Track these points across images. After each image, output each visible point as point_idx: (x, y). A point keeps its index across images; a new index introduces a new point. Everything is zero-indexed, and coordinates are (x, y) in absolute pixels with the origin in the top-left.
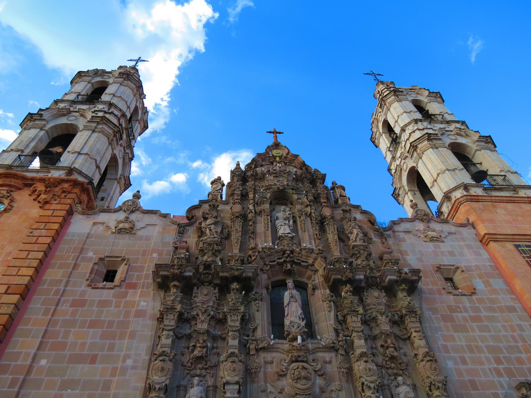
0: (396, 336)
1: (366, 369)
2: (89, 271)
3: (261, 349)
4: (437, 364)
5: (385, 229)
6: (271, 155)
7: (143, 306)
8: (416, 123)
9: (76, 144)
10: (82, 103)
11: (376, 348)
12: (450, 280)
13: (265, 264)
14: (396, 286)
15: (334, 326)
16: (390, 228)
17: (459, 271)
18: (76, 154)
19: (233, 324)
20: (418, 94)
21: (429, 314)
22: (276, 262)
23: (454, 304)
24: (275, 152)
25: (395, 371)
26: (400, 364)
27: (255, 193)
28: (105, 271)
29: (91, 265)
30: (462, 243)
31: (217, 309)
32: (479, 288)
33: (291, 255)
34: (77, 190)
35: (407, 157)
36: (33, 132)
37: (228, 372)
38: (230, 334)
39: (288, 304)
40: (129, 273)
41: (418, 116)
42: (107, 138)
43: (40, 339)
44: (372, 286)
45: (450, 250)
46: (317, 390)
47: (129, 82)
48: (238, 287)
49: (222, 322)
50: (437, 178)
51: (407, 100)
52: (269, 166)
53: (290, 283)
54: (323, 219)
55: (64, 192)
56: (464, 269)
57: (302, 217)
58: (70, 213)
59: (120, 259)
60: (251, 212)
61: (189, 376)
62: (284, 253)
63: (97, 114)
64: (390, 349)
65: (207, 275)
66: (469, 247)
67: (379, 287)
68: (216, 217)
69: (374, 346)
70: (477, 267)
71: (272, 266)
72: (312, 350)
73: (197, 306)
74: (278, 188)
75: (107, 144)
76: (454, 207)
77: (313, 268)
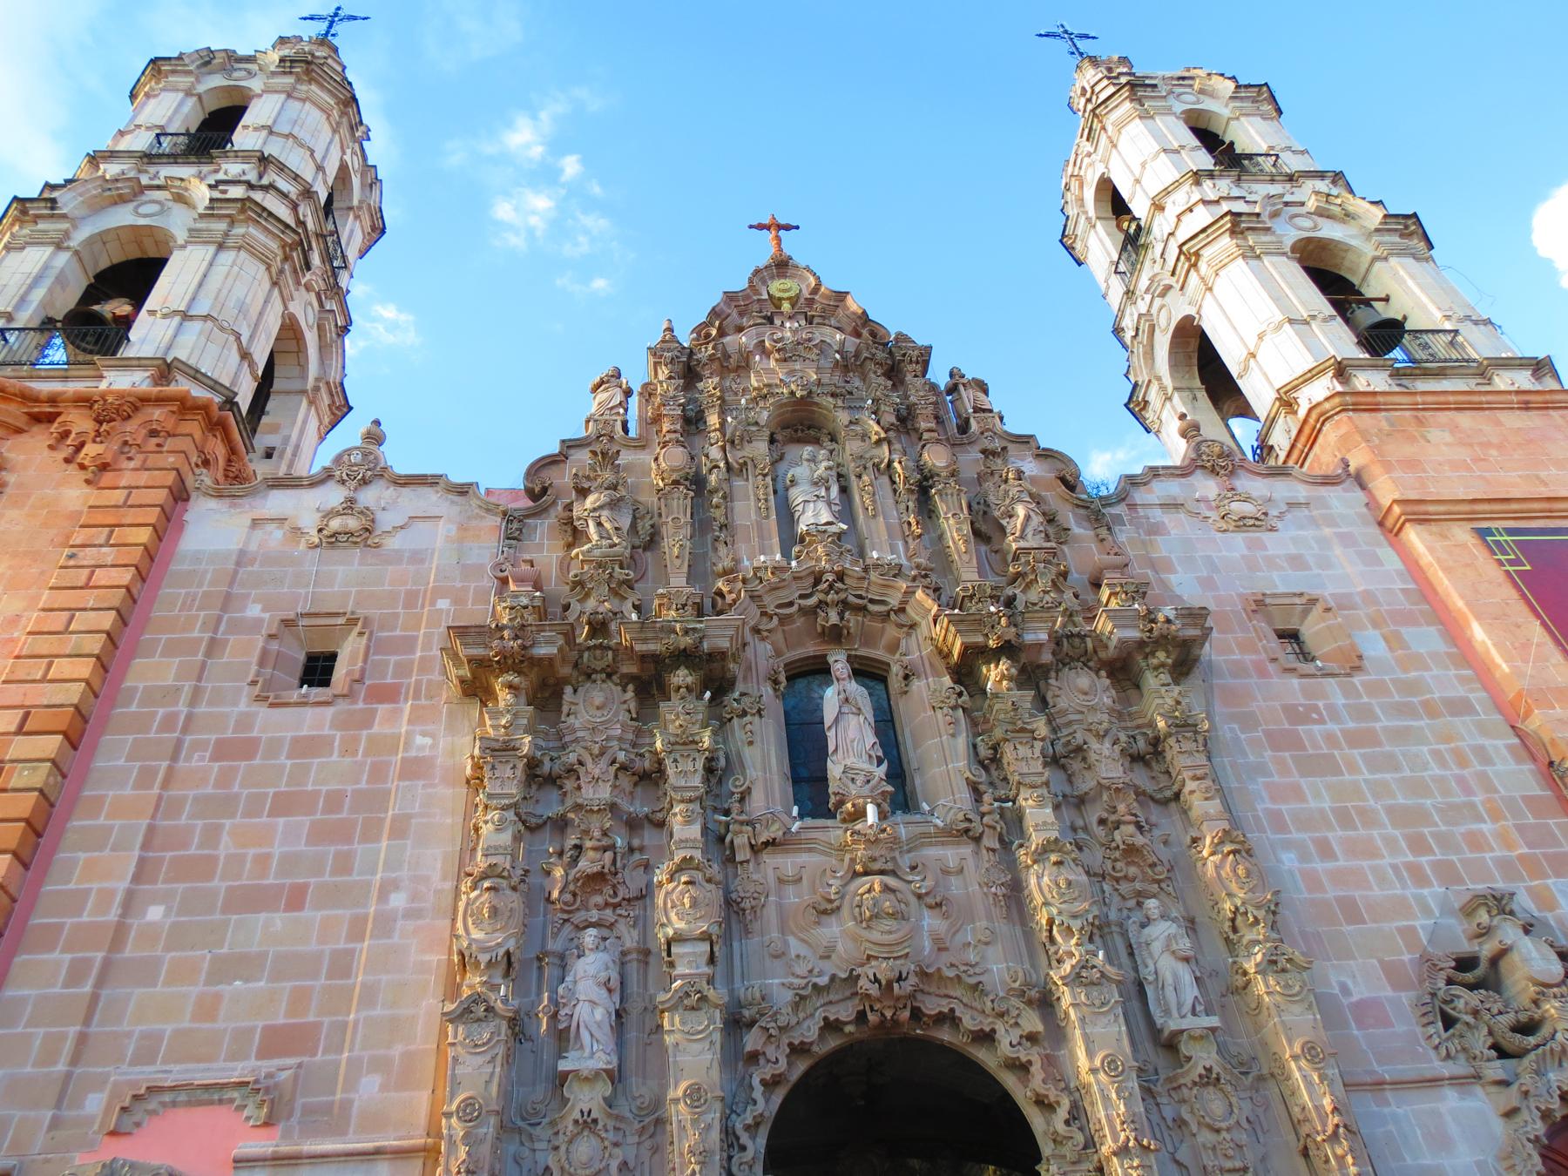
0: (1140, 794)
1: (1058, 885)
2: (255, 659)
3: (766, 844)
4: (1253, 860)
5: (1107, 501)
6: (765, 296)
7: (422, 748)
8: (1198, 183)
9: (168, 289)
10: (173, 158)
11: (1085, 829)
12: (1290, 636)
13: (764, 614)
14: (1139, 658)
15: (968, 774)
16: (1121, 497)
17: (1317, 610)
18: (177, 319)
19: (683, 784)
20: (1202, 91)
21: (1232, 730)
22: (796, 607)
23: (1302, 701)
24: (776, 287)
25: (1138, 886)
26: (1153, 866)
27: (722, 414)
28: (302, 657)
29: (260, 642)
30: (1327, 531)
31: (634, 745)
32: (1372, 653)
33: (839, 585)
35: (1169, 288)
36: (34, 258)
37: (678, 910)
38: (676, 809)
39: (837, 720)
40: (372, 658)
41: (1205, 160)
42: (263, 267)
43: (137, 853)
44: (1072, 659)
45: (1293, 550)
46: (927, 944)
47: (313, 87)
48: (689, 679)
49: (652, 777)
50: (1257, 346)
51: (1169, 111)
52: (761, 329)
53: (839, 664)
54: (926, 479)
55: (153, 433)
56: (1332, 604)
57: (865, 478)
58: (180, 495)
59: (341, 621)
60: (717, 467)
61: (568, 928)
62: (817, 581)
63: (225, 192)
64: (1122, 827)
65: (598, 652)
66: (1347, 540)
67: (1091, 664)
68: (614, 487)
69: (1080, 823)
70: (1368, 597)
71: (783, 620)
72: (909, 840)
73: (576, 740)
74: (792, 393)
75: (267, 285)
76: (1307, 430)
77: (902, 619)
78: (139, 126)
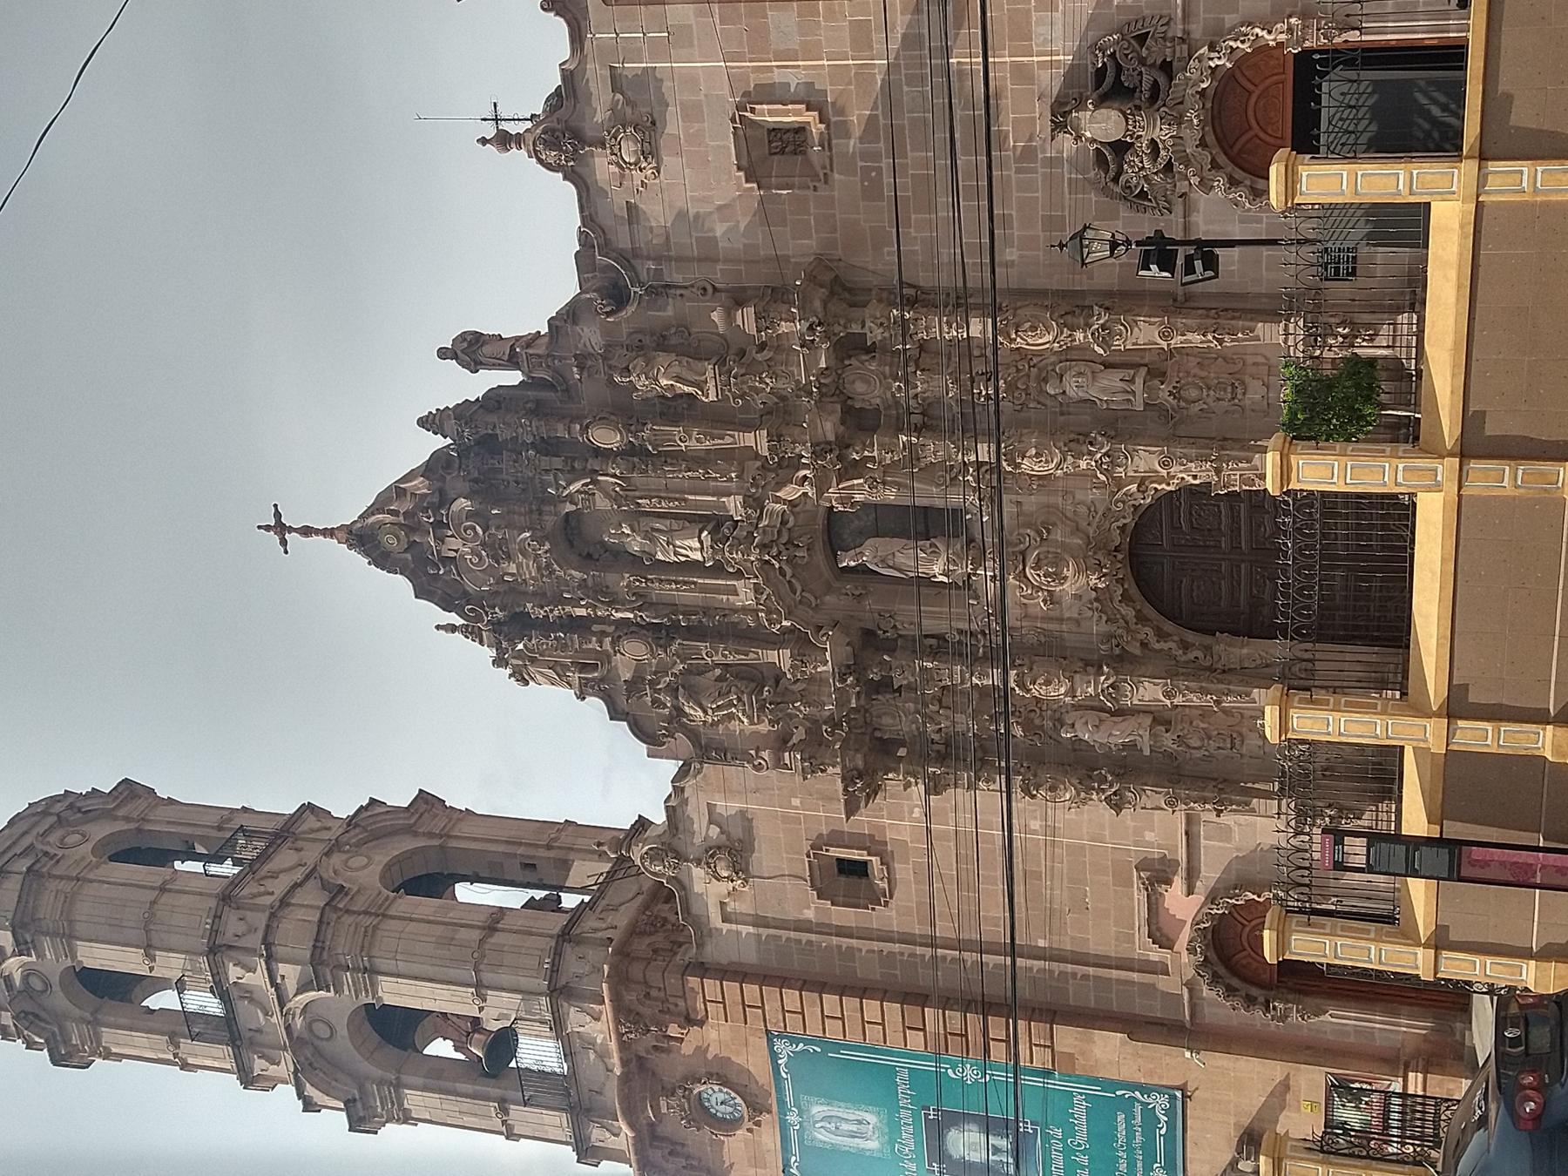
28: (843, 879)
34: (636, 971)
78: (175, 1056)
